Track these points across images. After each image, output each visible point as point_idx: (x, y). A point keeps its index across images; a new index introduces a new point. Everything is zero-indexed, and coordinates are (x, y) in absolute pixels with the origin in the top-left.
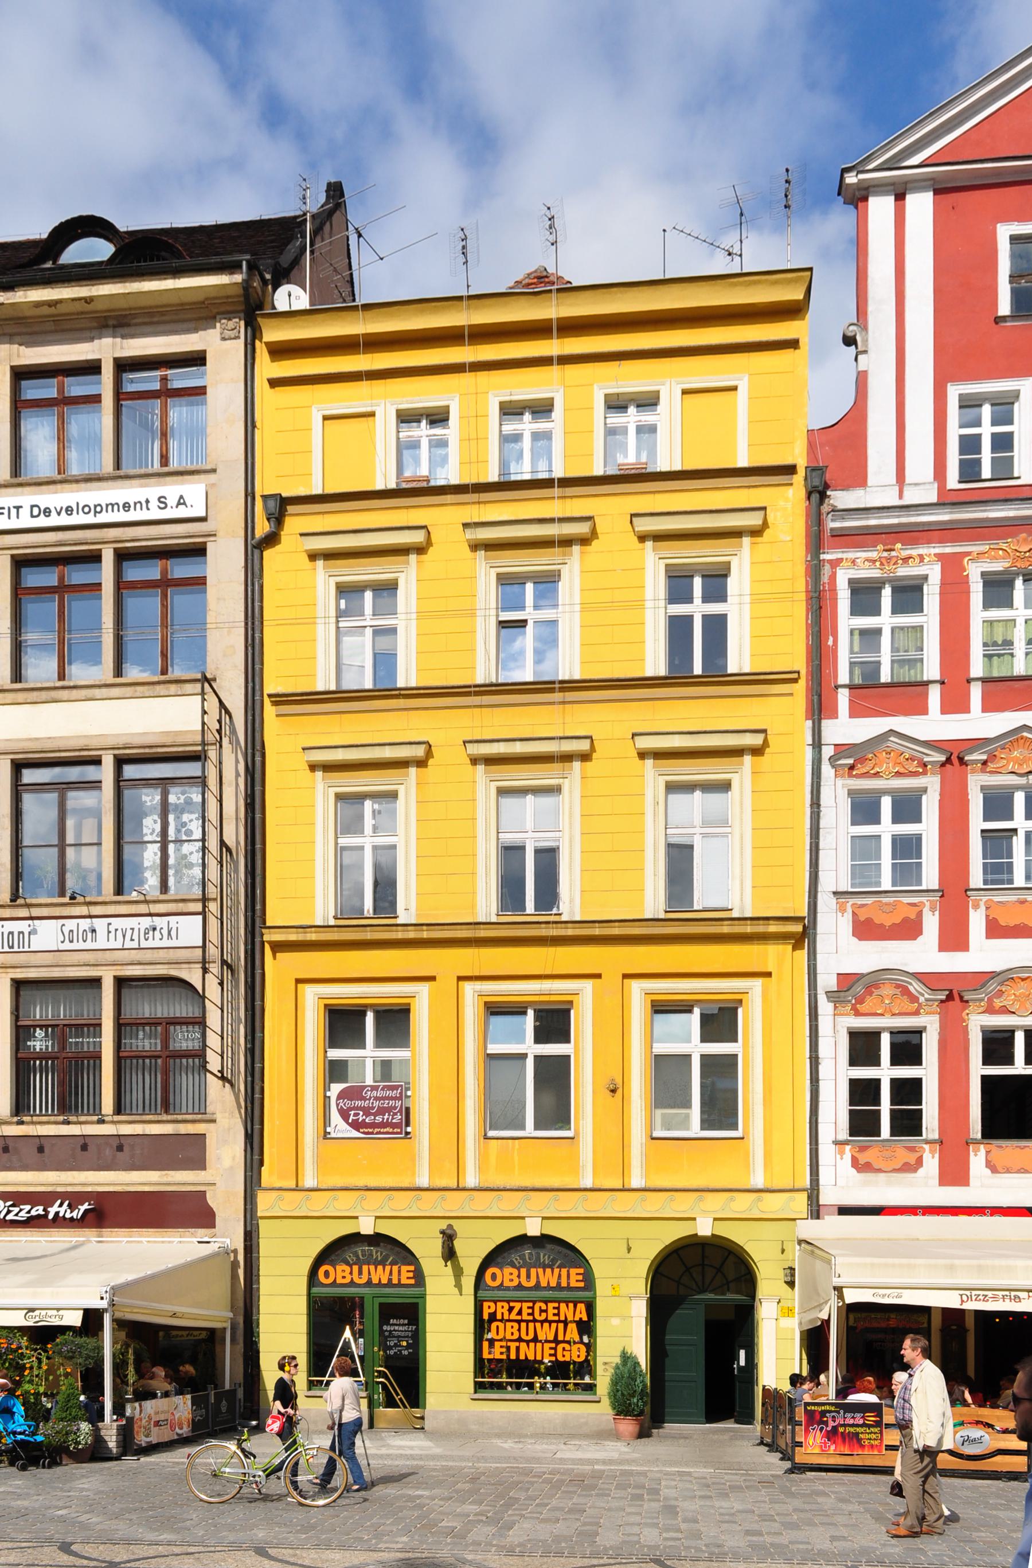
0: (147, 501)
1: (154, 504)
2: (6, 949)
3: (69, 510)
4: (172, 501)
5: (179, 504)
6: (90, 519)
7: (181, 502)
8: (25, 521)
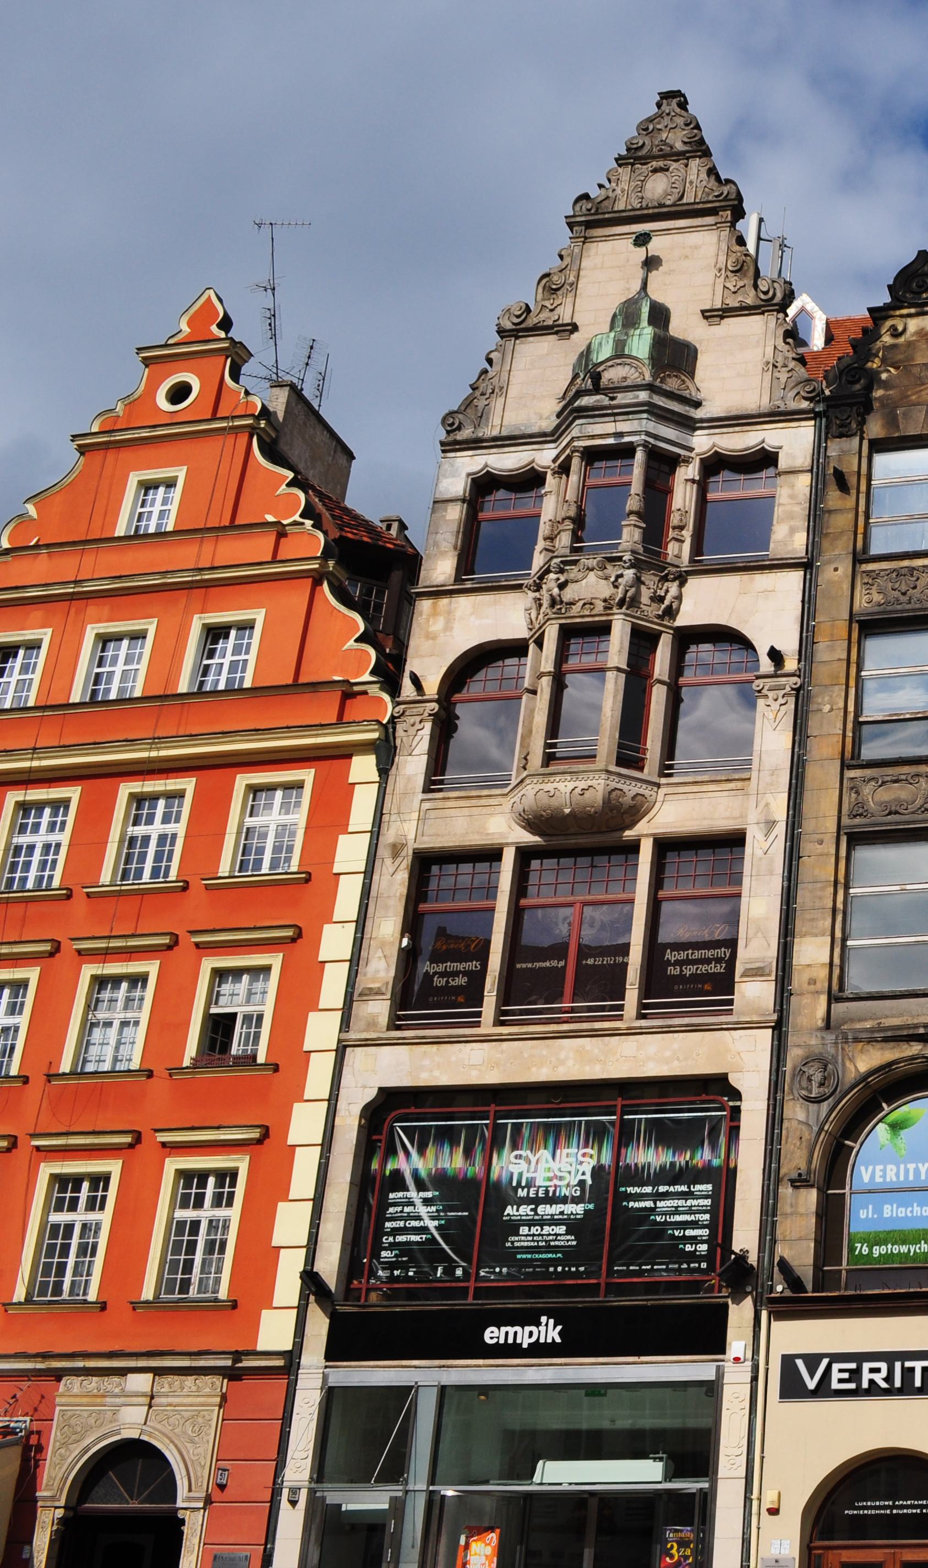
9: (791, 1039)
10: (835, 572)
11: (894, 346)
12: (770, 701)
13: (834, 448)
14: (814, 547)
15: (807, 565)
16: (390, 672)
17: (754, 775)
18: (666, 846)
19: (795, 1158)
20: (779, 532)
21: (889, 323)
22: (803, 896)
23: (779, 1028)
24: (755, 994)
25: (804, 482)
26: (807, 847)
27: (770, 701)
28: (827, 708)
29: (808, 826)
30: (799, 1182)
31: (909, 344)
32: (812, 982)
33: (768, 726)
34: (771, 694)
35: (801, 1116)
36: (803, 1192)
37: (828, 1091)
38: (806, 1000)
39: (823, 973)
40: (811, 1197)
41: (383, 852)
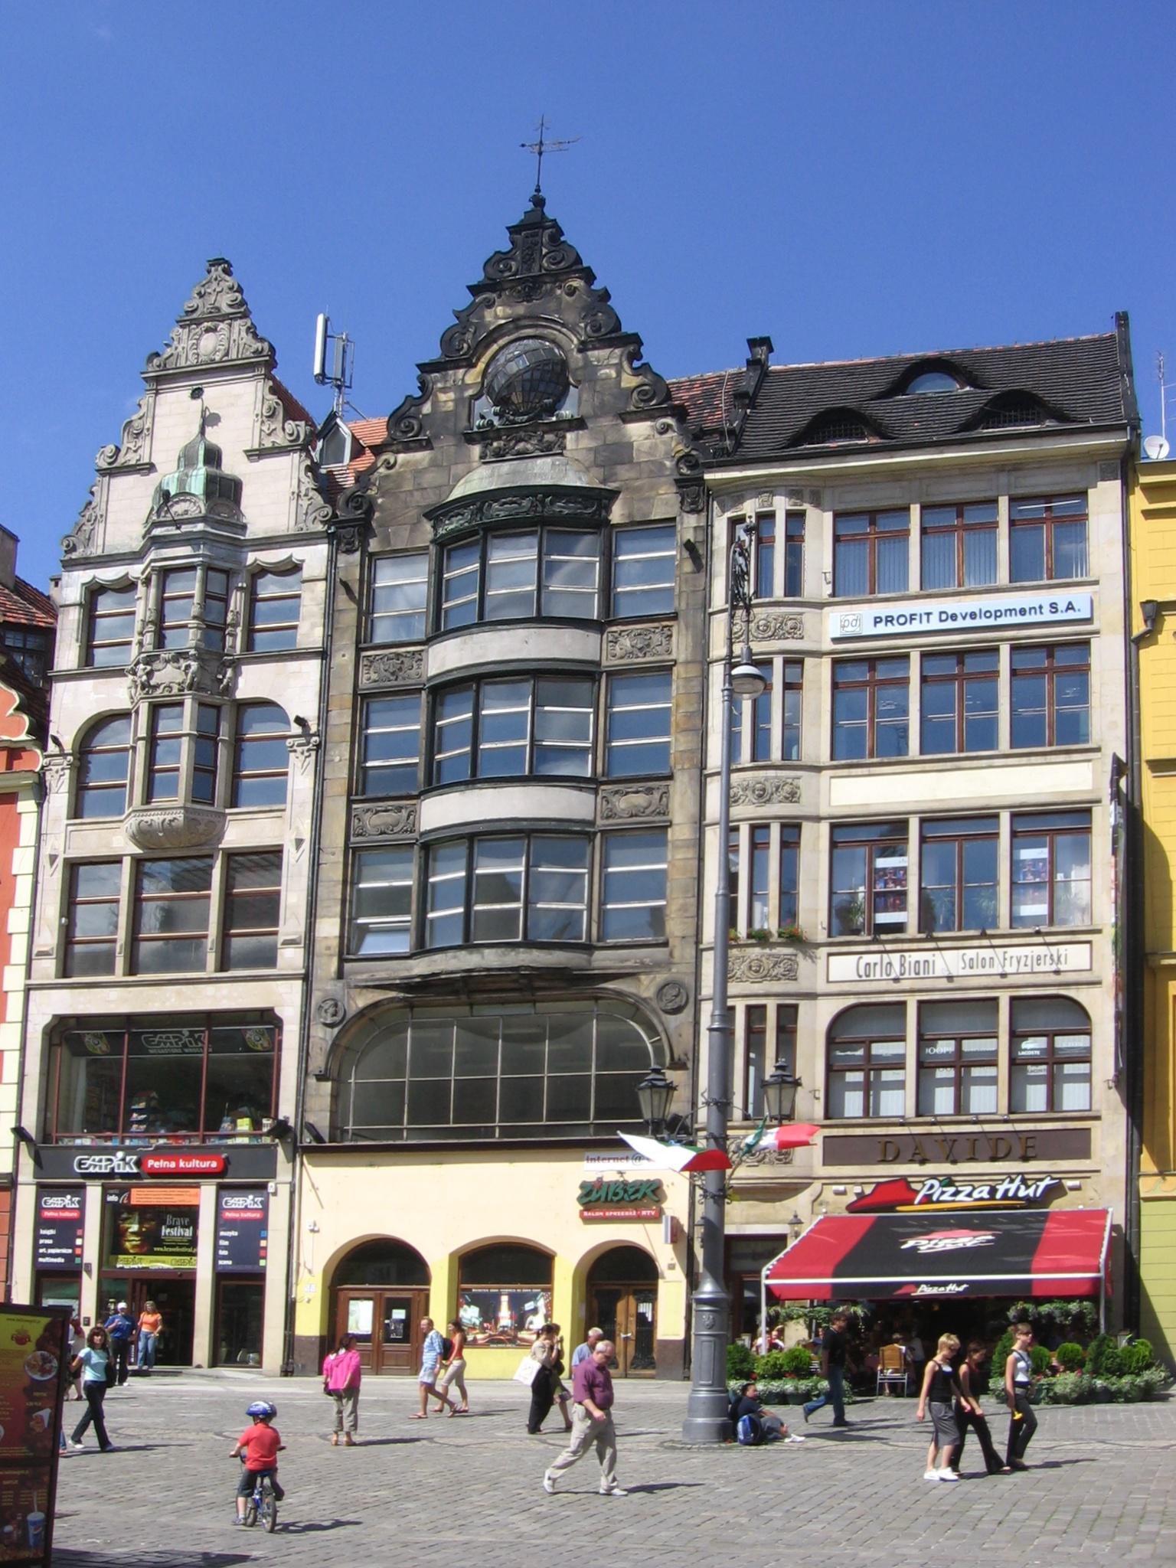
0: (1041, 607)
1: (1046, 609)
2: (913, 975)
3: (973, 616)
4: (1062, 606)
5: (1068, 609)
6: (991, 622)
7: (1070, 607)
8: (935, 624)
9: (314, 986)
10: (344, 658)
11: (387, 476)
12: (298, 754)
13: (343, 560)
14: (329, 637)
15: (324, 654)
16: (40, 731)
17: (288, 806)
18: (231, 855)
19: (318, 1062)
20: (304, 627)
21: (384, 457)
22: (322, 892)
23: (307, 978)
24: (291, 958)
25: (322, 586)
26: (324, 858)
27: (298, 754)
28: (337, 759)
29: (325, 842)
30: (321, 1078)
31: (399, 474)
32: (328, 948)
33: (298, 771)
34: (299, 749)
35: (321, 1035)
36: (323, 1084)
37: (337, 1019)
38: (324, 960)
39: (335, 943)
40: (328, 1086)
41: (44, 861)
